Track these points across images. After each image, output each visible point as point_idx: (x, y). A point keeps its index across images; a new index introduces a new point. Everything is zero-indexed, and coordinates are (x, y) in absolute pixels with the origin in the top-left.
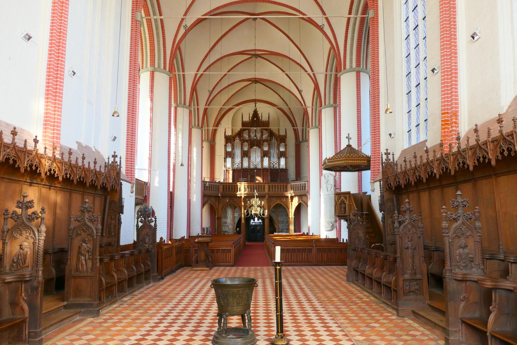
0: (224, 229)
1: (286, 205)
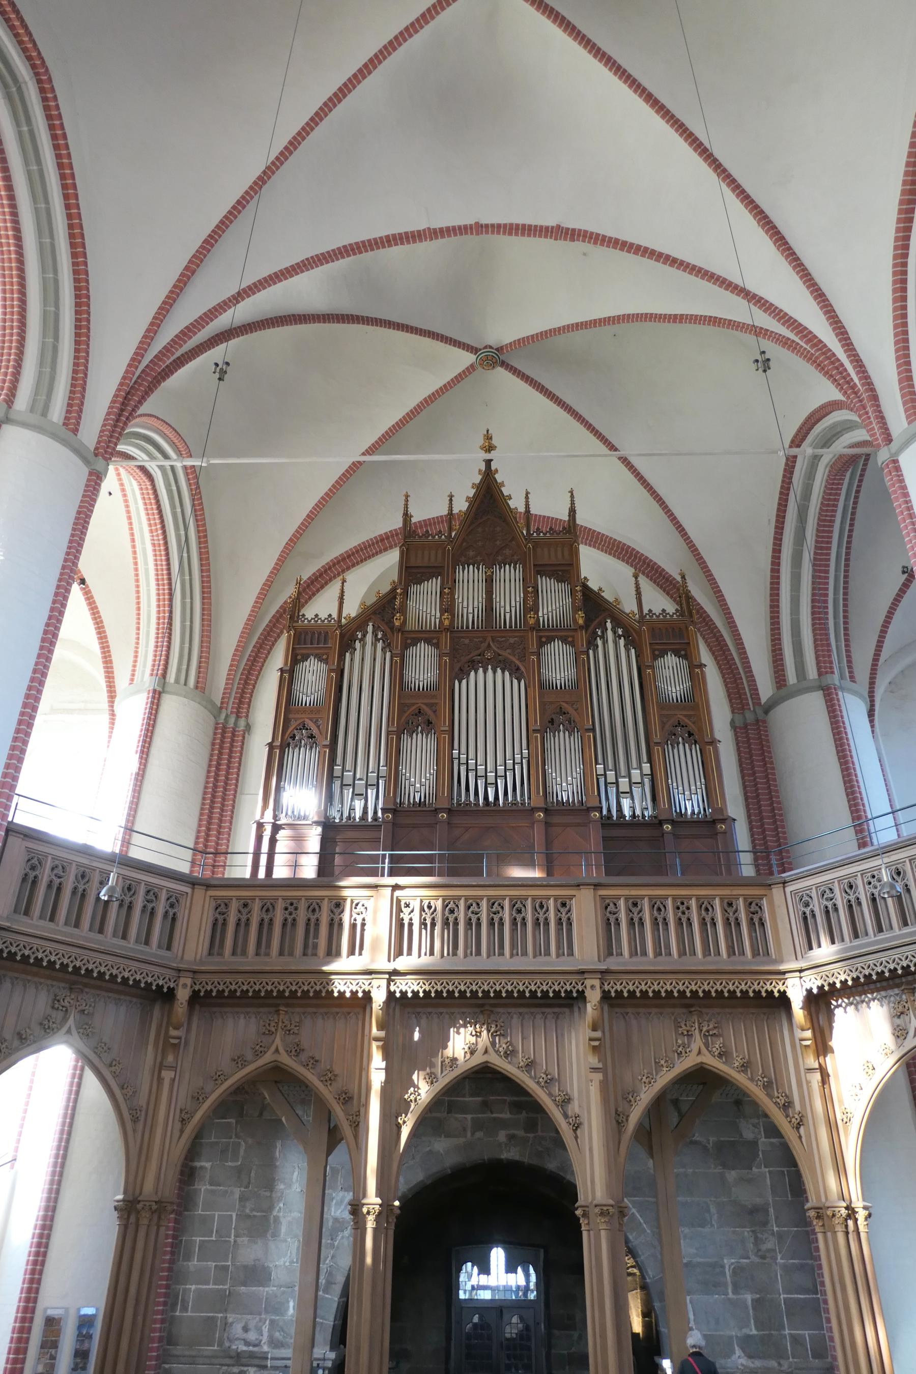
0: (237, 1330)
1: (768, 1086)
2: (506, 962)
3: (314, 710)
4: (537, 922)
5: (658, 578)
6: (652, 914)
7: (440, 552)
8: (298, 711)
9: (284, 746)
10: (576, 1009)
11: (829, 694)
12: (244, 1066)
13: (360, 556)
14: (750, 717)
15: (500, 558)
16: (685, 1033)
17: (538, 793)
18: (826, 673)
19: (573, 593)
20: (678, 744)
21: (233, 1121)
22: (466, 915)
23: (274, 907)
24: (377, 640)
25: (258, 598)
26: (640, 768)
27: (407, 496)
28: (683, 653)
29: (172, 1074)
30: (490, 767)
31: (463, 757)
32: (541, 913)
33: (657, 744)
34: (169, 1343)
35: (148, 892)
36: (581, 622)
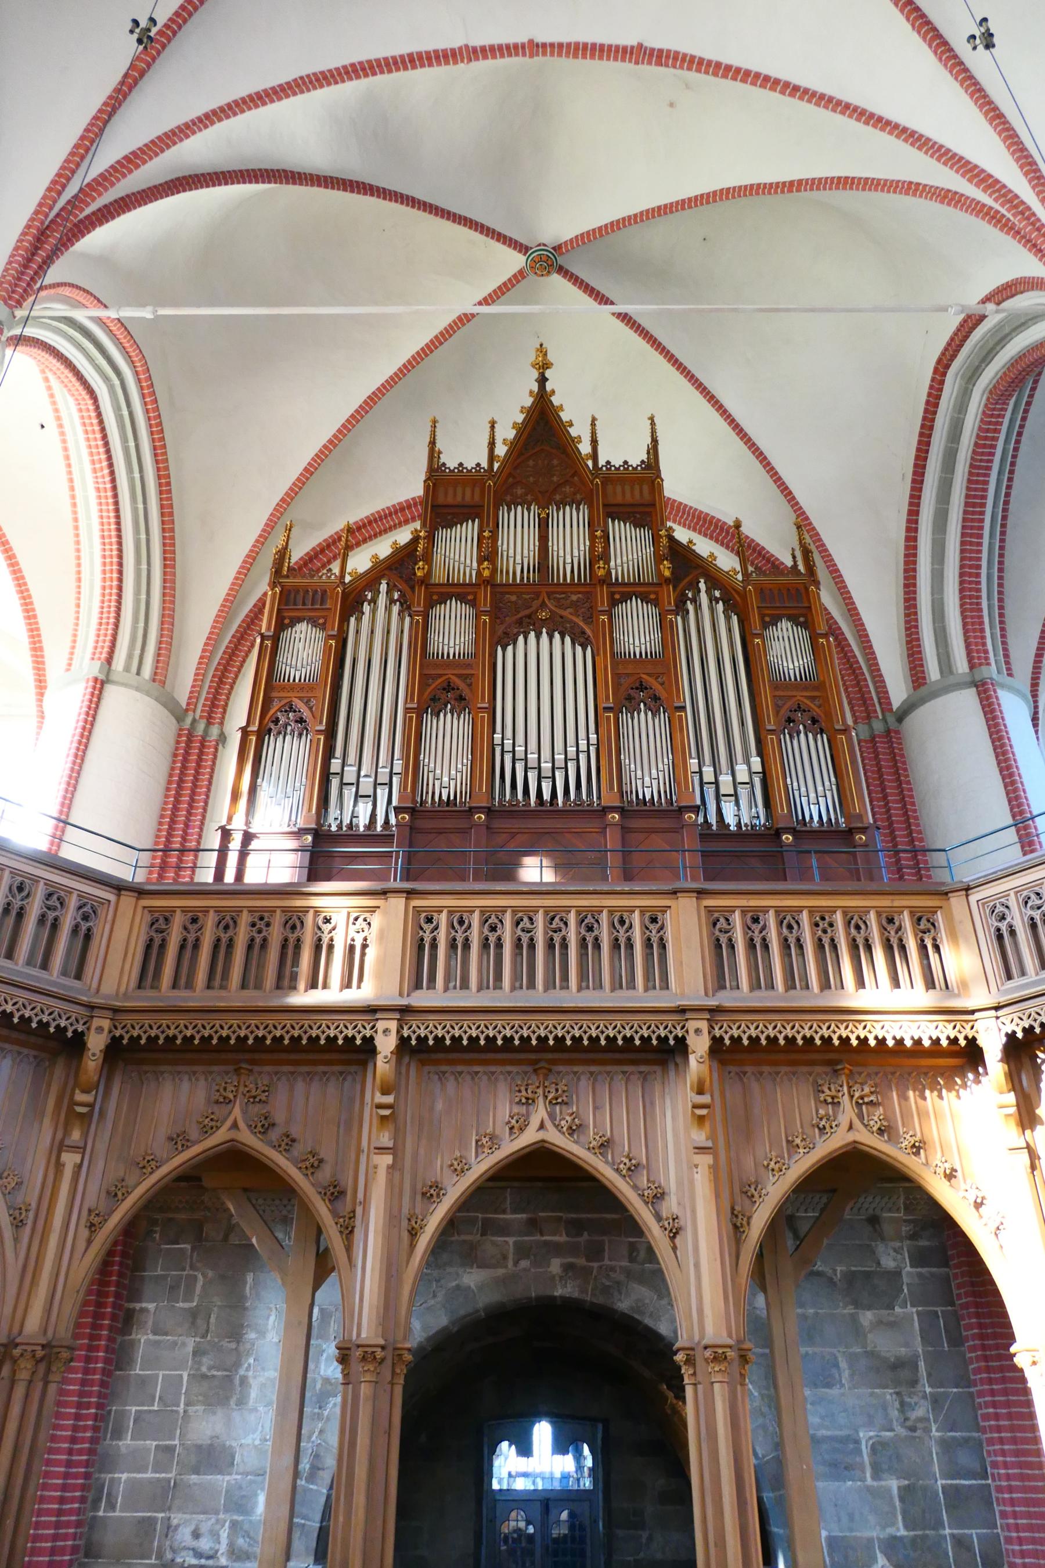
0: (184, 1535)
2: (572, 997)
3: (305, 688)
4: (615, 945)
5: (757, 558)
6: (780, 934)
7: (477, 490)
8: (283, 689)
9: (263, 733)
10: (672, 1066)
11: (986, 691)
12: (185, 1147)
13: (373, 529)
14: (878, 726)
15: (558, 497)
16: (829, 1100)
17: (612, 788)
18: (981, 664)
19: (656, 540)
20: (798, 733)
21: (188, 1247)
22: (514, 933)
23: (235, 922)
24: (392, 602)
25: (239, 573)
26: (748, 763)
27: (435, 422)
28: (802, 619)
29: (77, 1158)
30: (546, 754)
31: (508, 743)
32: (622, 931)
33: (772, 731)
34: (86, 1556)
35: (49, 896)
36: (667, 573)
